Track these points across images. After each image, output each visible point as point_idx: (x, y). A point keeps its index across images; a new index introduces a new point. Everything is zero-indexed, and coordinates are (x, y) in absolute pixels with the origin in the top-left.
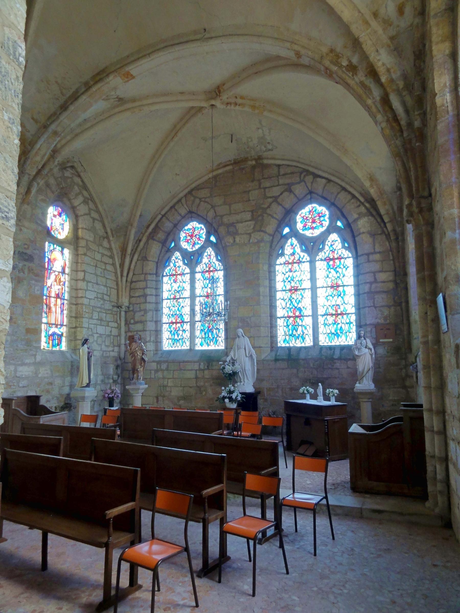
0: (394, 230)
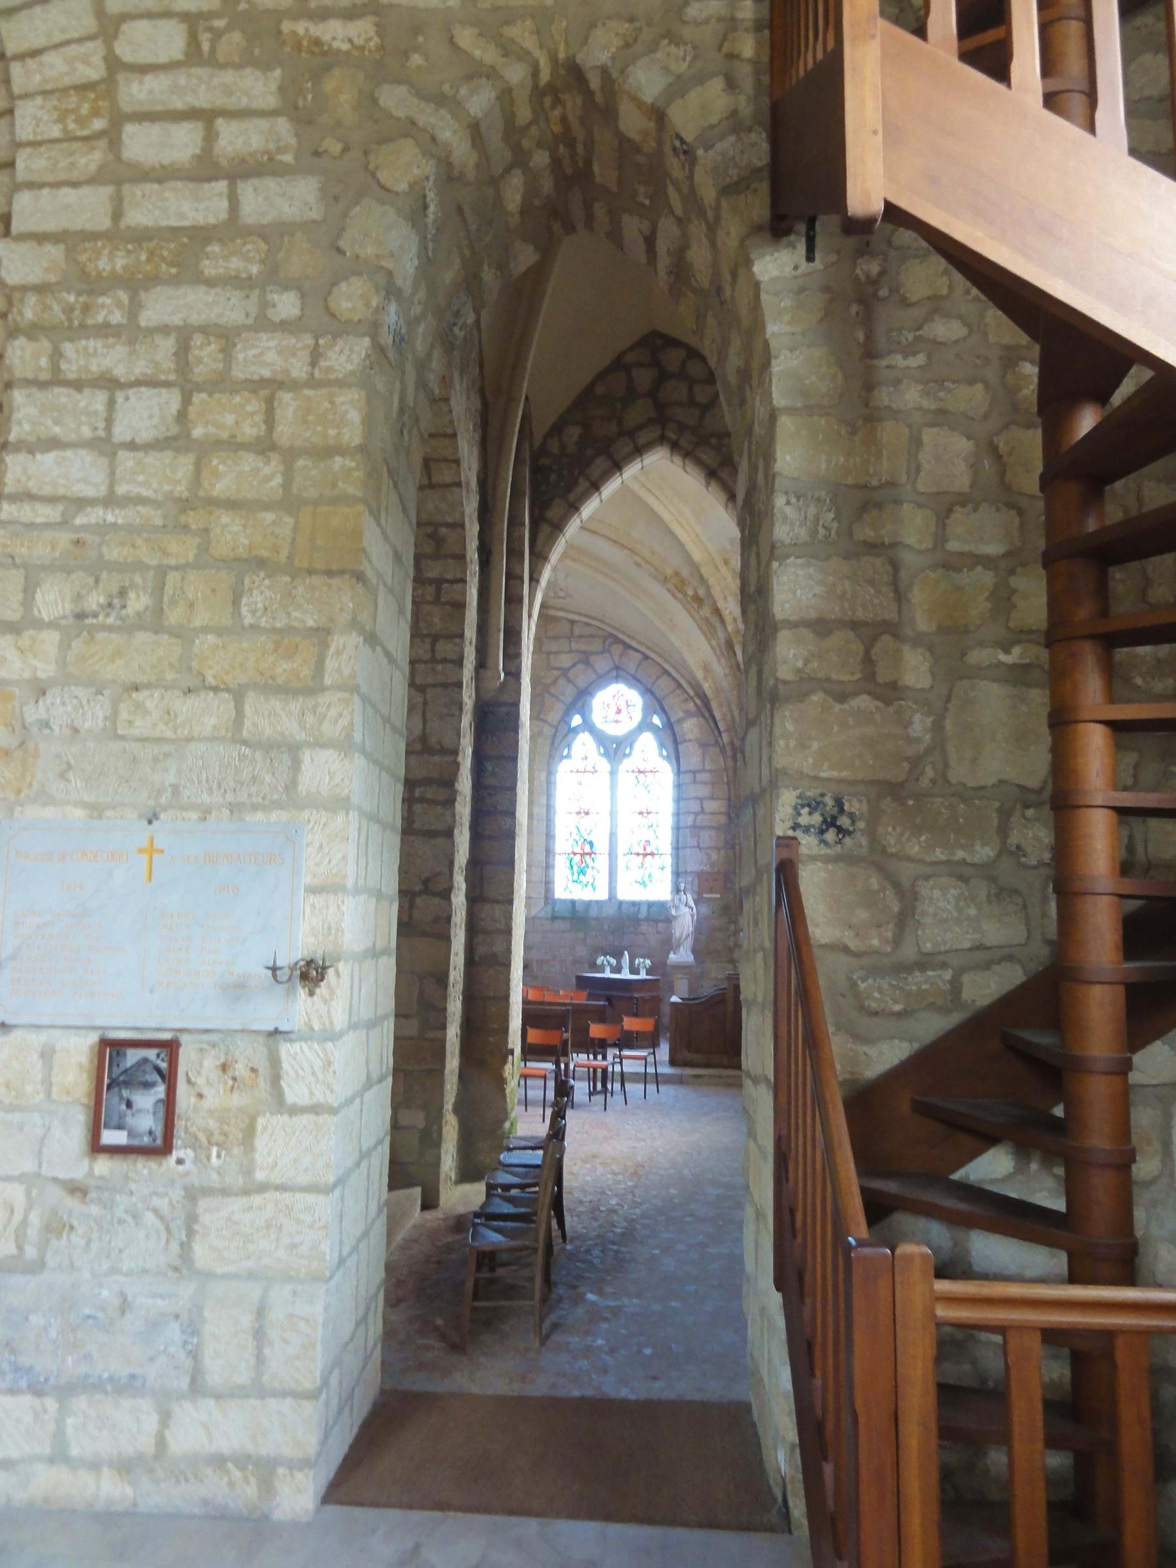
0: (732, 744)
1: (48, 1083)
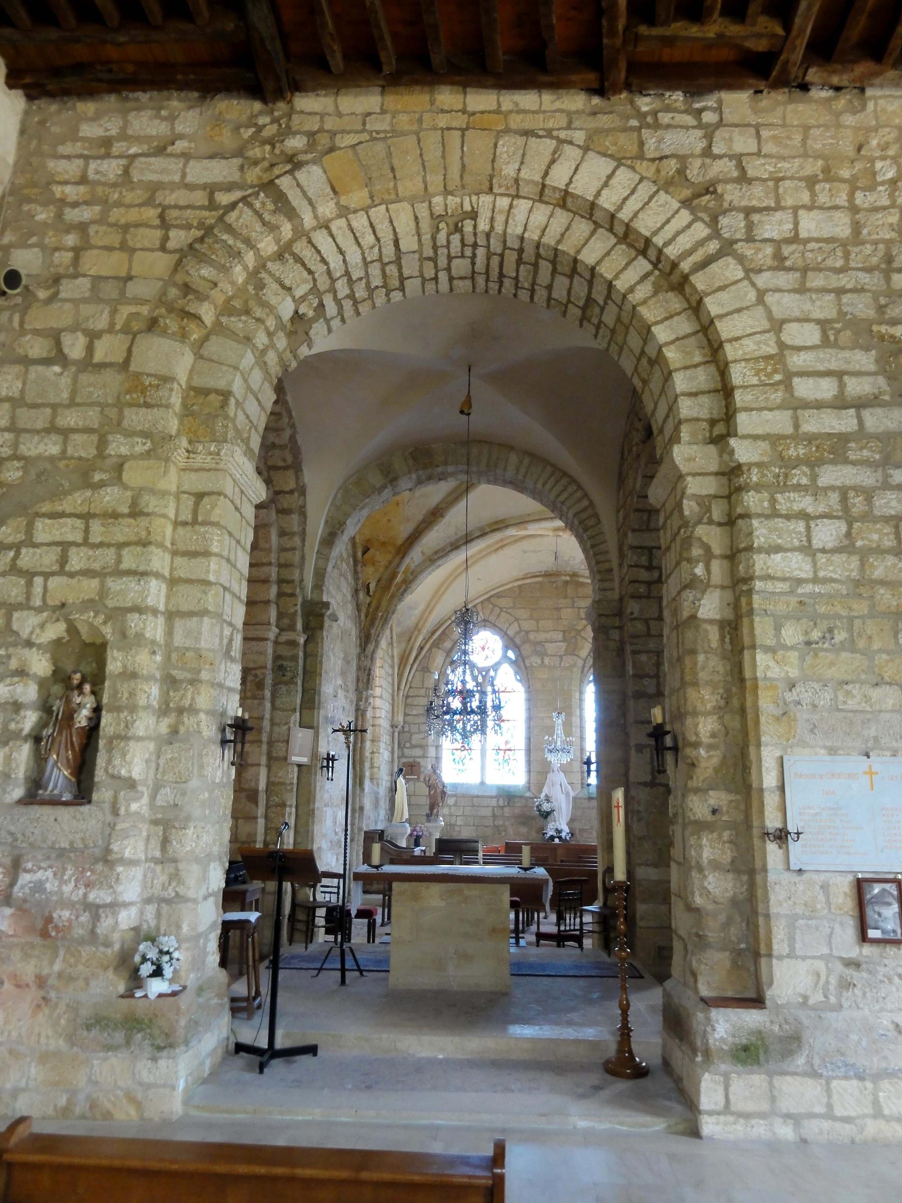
1: (828, 903)
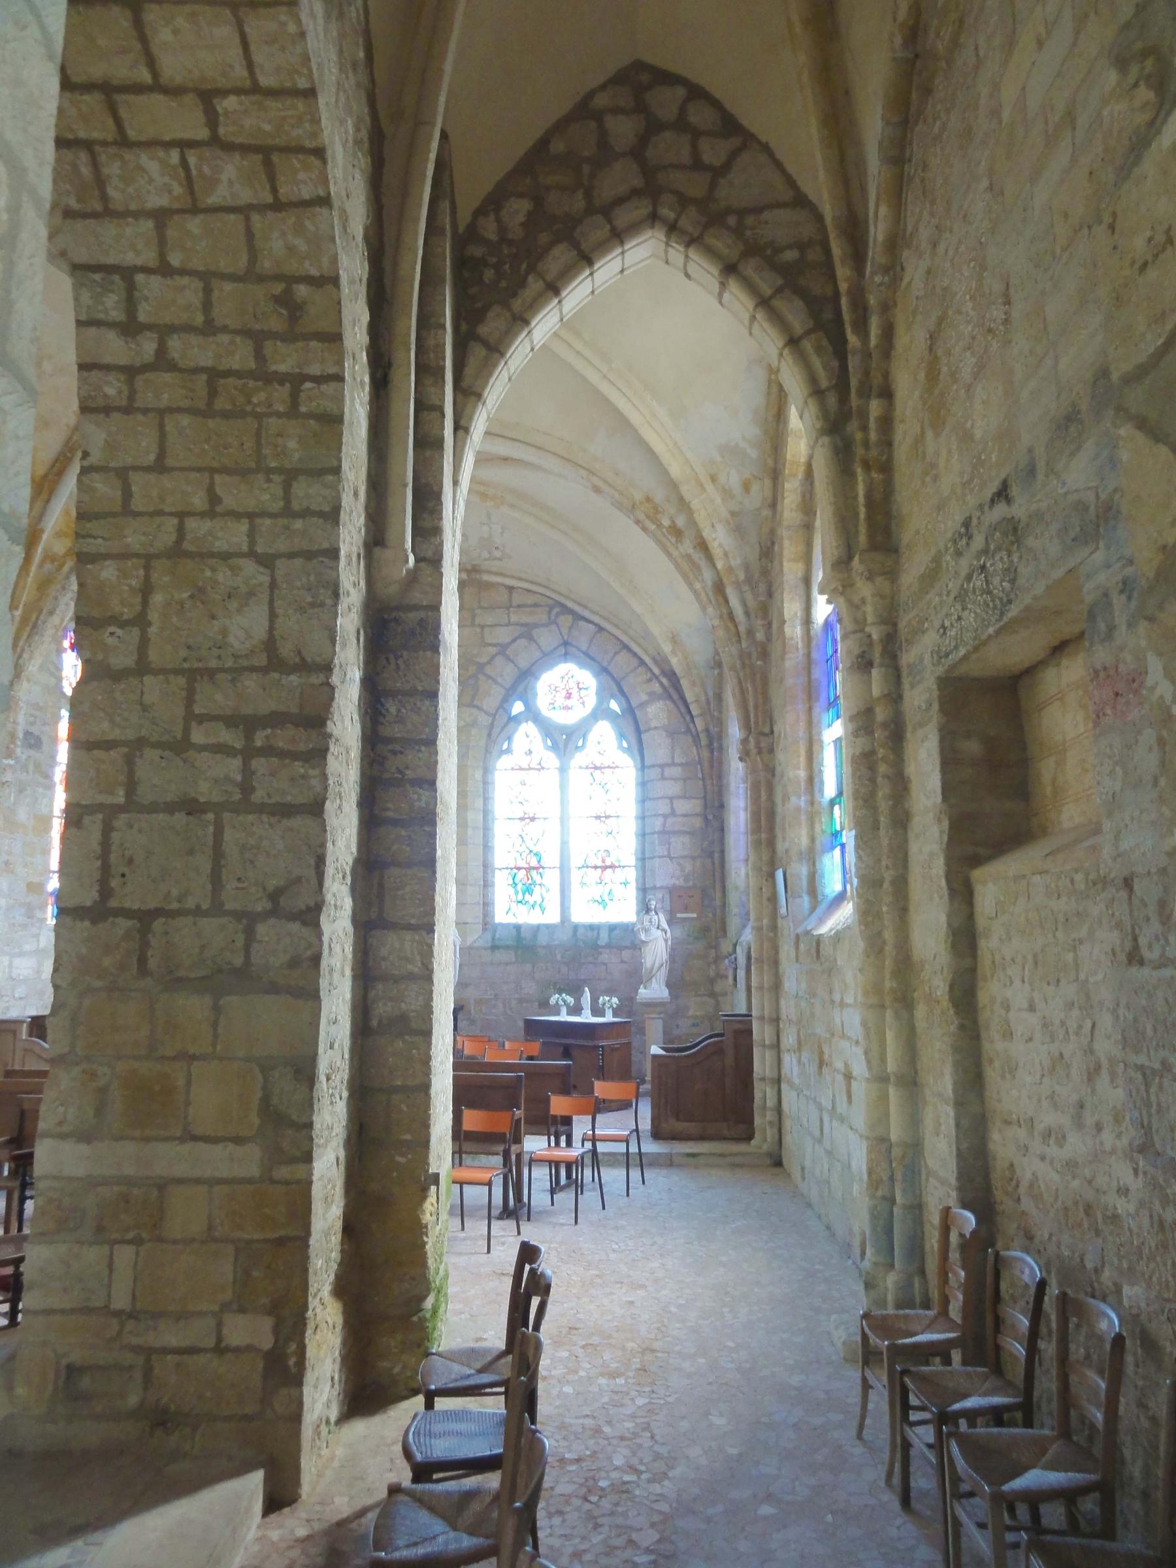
0: (707, 730)
